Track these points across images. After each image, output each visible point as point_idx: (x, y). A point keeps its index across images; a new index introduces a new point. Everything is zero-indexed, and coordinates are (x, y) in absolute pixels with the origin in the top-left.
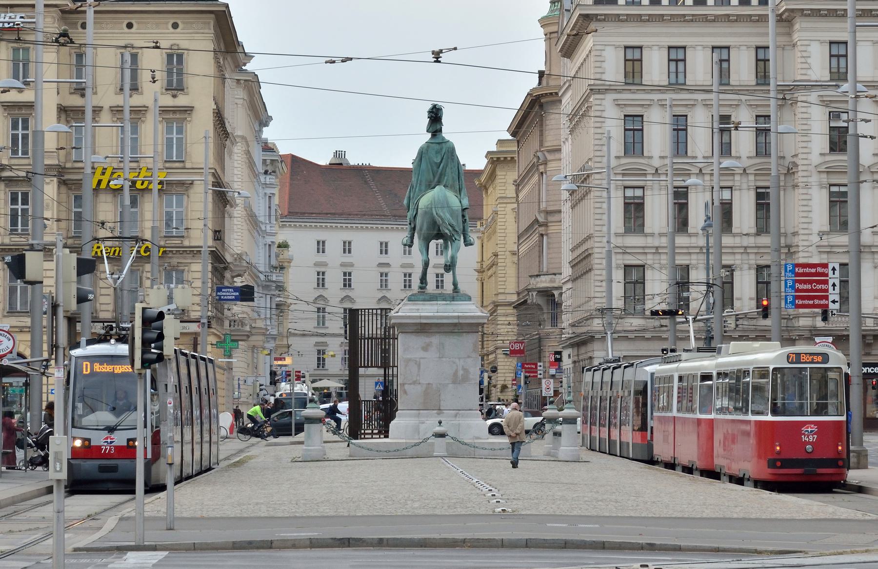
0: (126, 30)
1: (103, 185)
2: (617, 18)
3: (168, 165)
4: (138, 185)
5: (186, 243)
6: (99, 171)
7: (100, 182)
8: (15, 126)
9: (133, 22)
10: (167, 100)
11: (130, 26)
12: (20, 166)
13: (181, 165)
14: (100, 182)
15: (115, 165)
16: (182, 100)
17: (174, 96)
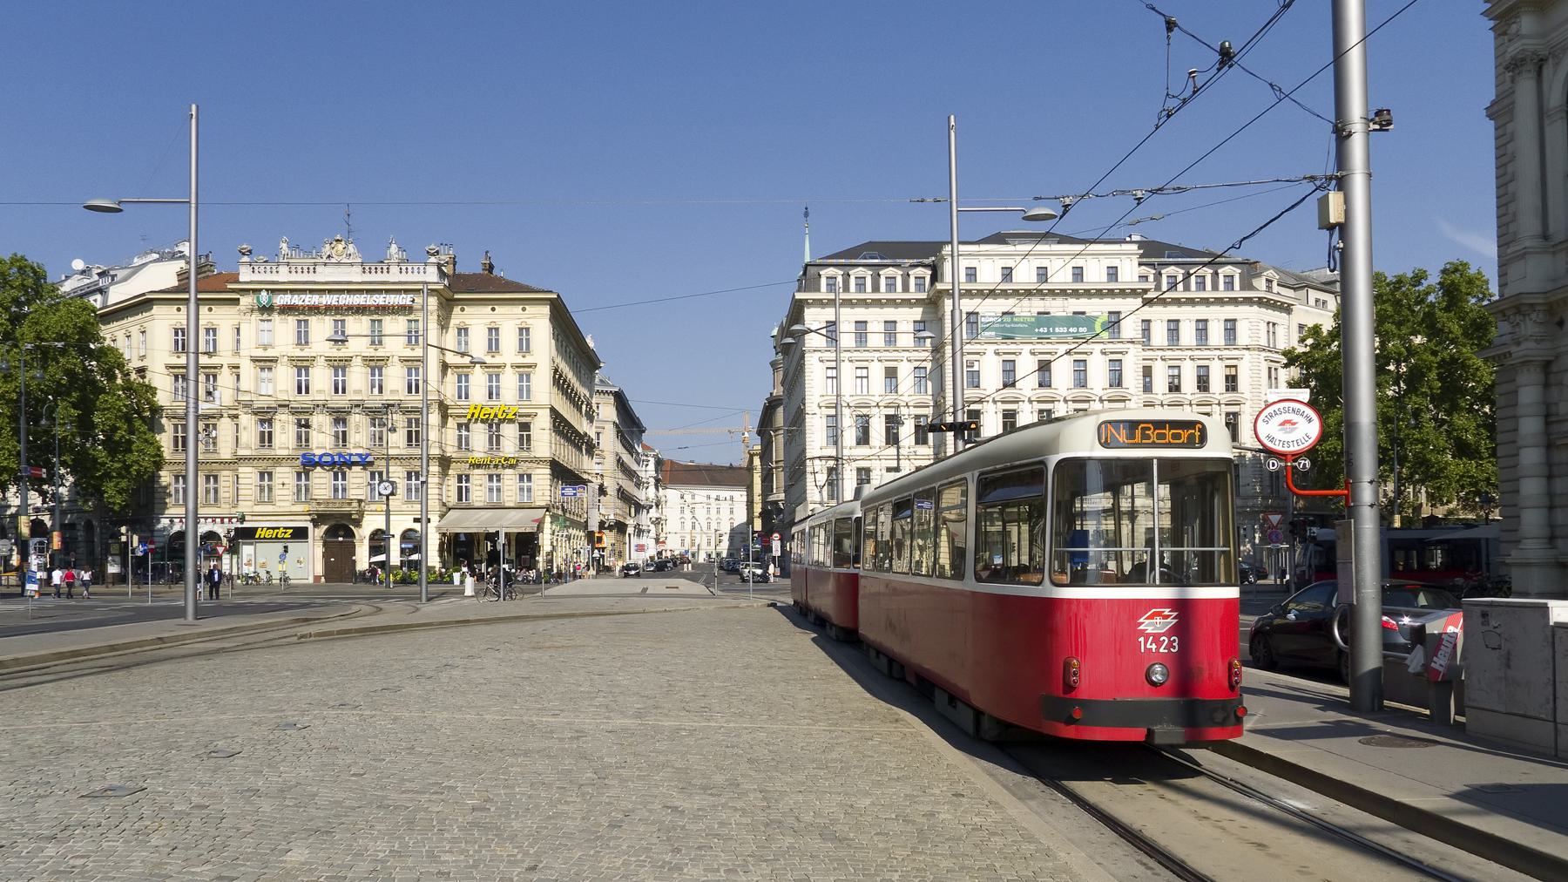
0: (492, 312)
1: (476, 416)
2: (820, 303)
3: (520, 403)
4: (499, 416)
5: (533, 455)
6: (472, 408)
7: (473, 414)
8: (410, 374)
9: (495, 307)
10: (520, 360)
11: (493, 309)
12: (415, 400)
13: (529, 403)
14: (473, 414)
15: (484, 404)
16: (529, 360)
17: (524, 357)
